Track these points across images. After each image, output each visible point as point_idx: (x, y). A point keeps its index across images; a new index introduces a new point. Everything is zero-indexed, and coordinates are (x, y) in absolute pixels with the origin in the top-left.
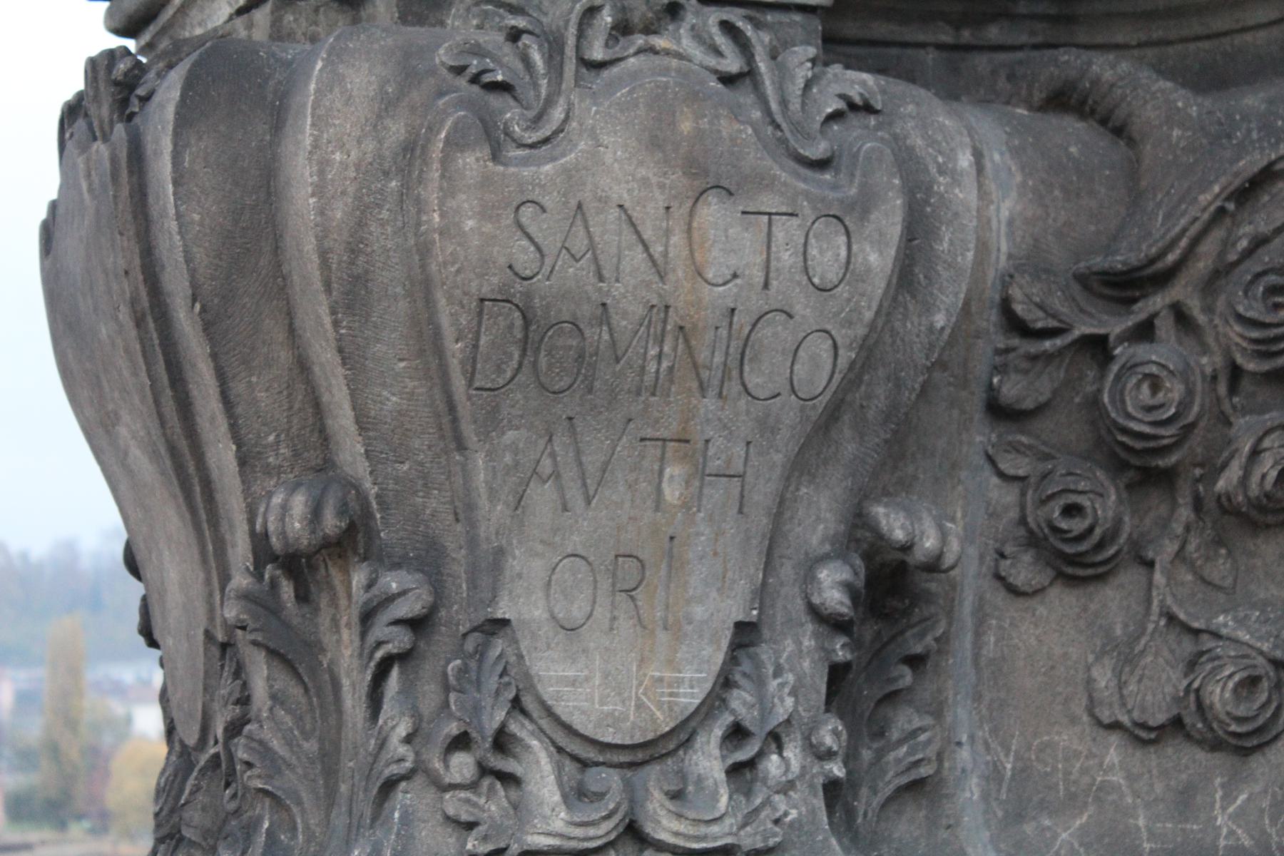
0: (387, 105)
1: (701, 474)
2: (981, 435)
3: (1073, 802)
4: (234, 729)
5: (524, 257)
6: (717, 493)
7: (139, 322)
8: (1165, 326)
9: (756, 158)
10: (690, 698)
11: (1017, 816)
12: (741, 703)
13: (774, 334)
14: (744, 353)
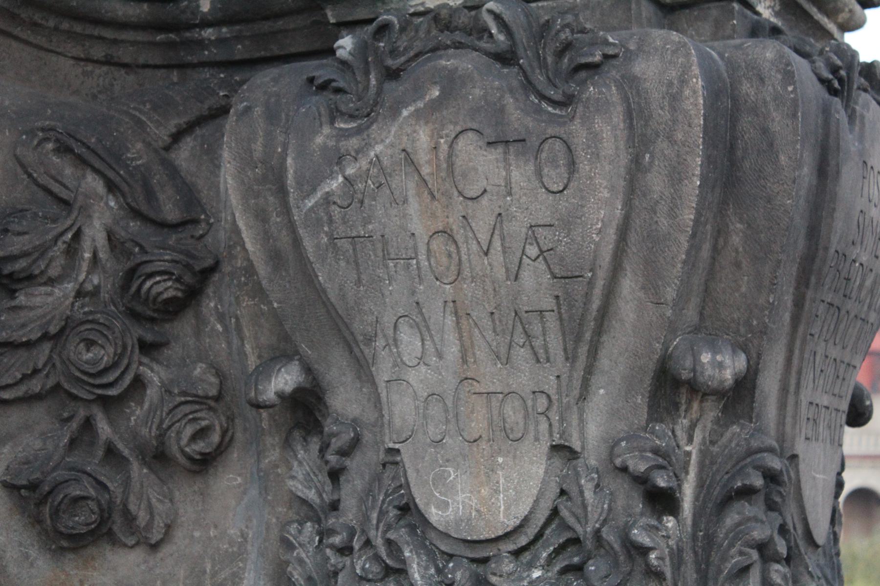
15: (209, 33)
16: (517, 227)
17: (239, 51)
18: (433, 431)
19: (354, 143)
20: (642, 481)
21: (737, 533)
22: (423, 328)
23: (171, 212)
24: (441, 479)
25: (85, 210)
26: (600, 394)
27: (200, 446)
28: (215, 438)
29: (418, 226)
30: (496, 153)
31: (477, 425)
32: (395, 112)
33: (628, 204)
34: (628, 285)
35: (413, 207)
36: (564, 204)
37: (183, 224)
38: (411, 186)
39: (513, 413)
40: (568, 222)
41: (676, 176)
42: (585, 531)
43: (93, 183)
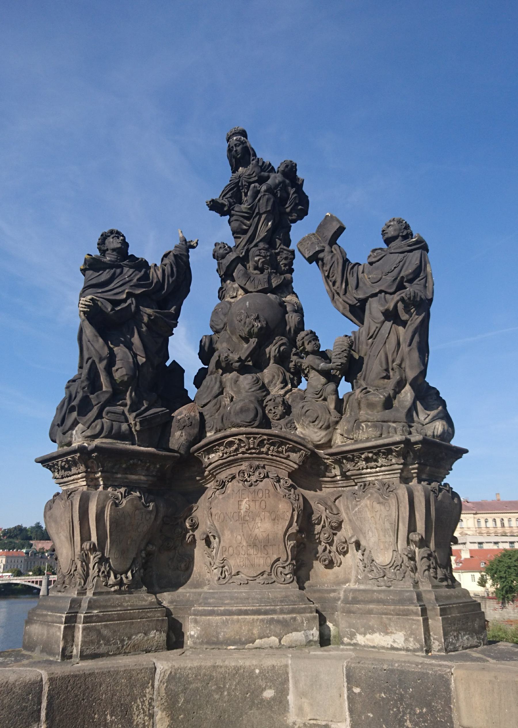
4: (75, 570)
7: (70, 523)
15: (340, 482)
16: (383, 516)
19: (358, 503)
23: (336, 513)
24: (378, 556)
28: (346, 548)
29: (369, 516)
30: (379, 505)
31: (382, 547)
32: (364, 498)
35: (368, 513)
37: (337, 514)
38: (367, 510)
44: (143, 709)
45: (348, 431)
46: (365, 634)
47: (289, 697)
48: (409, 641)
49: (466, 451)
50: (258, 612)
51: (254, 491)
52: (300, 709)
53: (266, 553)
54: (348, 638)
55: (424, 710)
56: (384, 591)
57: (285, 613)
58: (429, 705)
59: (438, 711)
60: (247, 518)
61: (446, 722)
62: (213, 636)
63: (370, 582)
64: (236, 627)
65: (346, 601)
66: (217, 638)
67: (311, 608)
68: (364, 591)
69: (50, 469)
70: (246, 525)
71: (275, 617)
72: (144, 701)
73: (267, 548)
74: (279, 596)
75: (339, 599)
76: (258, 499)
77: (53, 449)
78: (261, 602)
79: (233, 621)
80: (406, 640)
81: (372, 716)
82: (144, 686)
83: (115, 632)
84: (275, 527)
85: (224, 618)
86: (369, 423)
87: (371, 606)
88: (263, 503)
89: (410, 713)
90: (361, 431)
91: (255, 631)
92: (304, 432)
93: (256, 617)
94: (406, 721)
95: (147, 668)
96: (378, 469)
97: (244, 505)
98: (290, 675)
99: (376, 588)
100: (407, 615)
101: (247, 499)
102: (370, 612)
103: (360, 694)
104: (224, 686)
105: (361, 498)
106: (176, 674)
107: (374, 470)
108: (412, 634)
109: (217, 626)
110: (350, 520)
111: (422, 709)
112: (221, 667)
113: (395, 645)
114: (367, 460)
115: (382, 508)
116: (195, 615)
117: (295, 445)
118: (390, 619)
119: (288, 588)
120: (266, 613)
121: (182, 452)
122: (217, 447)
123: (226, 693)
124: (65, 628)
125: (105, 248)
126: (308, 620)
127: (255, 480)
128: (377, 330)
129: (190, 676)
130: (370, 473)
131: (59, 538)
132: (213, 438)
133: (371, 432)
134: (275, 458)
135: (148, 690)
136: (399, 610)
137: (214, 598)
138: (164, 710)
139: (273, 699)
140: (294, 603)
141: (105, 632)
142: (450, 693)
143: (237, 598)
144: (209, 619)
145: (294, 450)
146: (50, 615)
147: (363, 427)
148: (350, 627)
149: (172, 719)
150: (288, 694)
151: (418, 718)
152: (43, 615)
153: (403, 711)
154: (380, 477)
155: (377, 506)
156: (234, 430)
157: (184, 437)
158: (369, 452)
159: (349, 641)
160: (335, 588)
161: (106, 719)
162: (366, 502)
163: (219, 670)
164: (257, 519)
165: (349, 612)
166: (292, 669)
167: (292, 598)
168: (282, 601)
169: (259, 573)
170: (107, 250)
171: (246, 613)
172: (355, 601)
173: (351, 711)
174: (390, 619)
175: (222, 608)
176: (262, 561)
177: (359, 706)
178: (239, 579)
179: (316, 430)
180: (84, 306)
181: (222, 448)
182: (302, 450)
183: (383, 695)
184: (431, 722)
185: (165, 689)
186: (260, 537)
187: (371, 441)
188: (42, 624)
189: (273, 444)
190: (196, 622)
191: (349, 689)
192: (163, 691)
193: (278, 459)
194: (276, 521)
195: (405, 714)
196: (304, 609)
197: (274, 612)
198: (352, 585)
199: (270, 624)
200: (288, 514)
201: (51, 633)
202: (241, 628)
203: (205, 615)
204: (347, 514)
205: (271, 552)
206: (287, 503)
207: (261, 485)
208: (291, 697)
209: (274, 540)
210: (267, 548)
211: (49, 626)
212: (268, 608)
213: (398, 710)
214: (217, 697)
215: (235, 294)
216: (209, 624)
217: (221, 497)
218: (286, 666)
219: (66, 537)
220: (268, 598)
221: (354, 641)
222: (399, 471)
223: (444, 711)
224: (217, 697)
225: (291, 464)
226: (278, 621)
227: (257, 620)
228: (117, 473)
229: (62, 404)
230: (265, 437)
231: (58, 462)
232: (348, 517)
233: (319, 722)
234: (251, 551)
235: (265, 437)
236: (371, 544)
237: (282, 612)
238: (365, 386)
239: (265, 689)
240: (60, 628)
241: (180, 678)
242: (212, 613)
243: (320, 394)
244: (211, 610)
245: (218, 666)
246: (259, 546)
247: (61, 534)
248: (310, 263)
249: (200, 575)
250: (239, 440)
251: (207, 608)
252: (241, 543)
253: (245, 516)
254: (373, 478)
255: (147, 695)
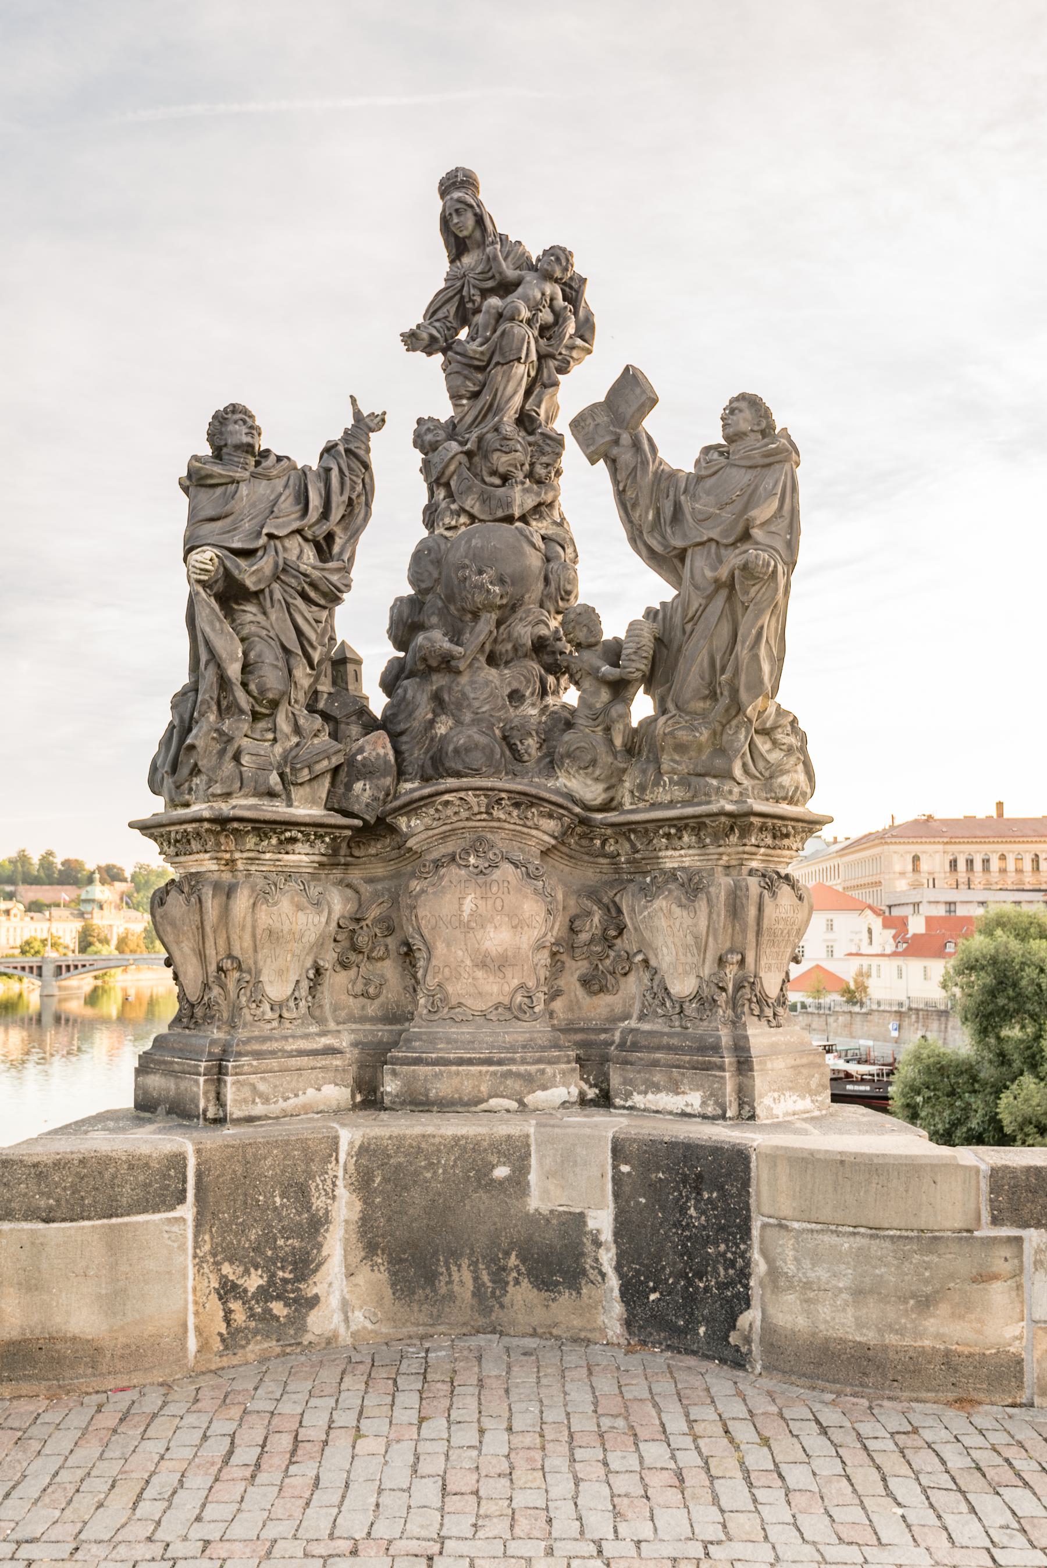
0: (250, 897)
1: (293, 955)
2: (333, 945)
3: (344, 1008)
5: (271, 922)
6: (296, 958)
8: (365, 928)
9: (307, 904)
10: (289, 993)
11: (335, 1011)
12: (297, 994)
13: (307, 933)
14: (302, 936)
16: (685, 926)
17: (632, 870)
18: (671, 971)
20: (717, 984)
21: (742, 996)
22: (667, 947)
25: (593, 915)
26: (707, 964)
27: (623, 972)
31: (680, 970)
33: (709, 921)
34: (711, 939)
36: (695, 920)
39: (688, 968)
40: (695, 925)
41: (719, 915)
42: (704, 996)
43: (595, 908)
44: (325, 1190)
45: (642, 788)
46: (646, 1093)
47: (529, 1177)
48: (708, 1105)
49: (831, 820)
50: (489, 1062)
51: (485, 883)
52: (545, 1193)
53: (501, 975)
54: (621, 1099)
55: (715, 1195)
56: (678, 1034)
57: (528, 1063)
58: (721, 1188)
59: (732, 1196)
60: (473, 925)
61: (742, 1209)
62: (421, 1094)
63: (660, 1020)
64: (455, 1081)
65: (622, 1046)
66: (427, 1096)
67: (568, 1056)
68: (650, 1033)
69: (156, 840)
70: (471, 935)
71: (514, 1068)
72: (325, 1180)
73: (503, 969)
74: (520, 1039)
75: (613, 1042)
76: (489, 895)
77: (155, 806)
78: (493, 1047)
79: (450, 1072)
80: (704, 1103)
81: (643, 1201)
82: (326, 1160)
83: (276, 1086)
84: (517, 938)
85: (437, 1069)
86: (675, 777)
87: (658, 1055)
88: (499, 902)
89: (695, 1199)
90: (661, 789)
91: (484, 1088)
92: (569, 784)
93: (484, 1068)
94: (690, 1208)
95: (328, 1137)
96: (682, 852)
97: (468, 905)
98: (533, 1148)
99: (667, 1030)
100: (707, 1070)
101: (473, 895)
102: (655, 1064)
103: (629, 1174)
104: (439, 1162)
105: (654, 896)
106: (369, 1144)
107: (677, 853)
108: (712, 1095)
109: (425, 1080)
110: (635, 929)
111: (711, 1193)
112: (434, 1136)
113: (688, 1110)
114: (668, 836)
115: (685, 913)
116: (392, 1064)
117: (553, 808)
118: (683, 1074)
119: (535, 1027)
120: (500, 1063)
121: (367, 817)
122: (424, 809)
123: (440, 1171)
124: (206, 1081)
125: (222, 443)
126: (564, 1073)
127: (486, 865)
128: (701, 608)
129: (390, 1147)
130: (671, 857)
131: (181, 949)
132: (417, 795)
133: (677, 793)
134: (519, 828)
135: (330, 1166)
136: (697, 1061)
137: (421, 1040)
138: (354, 1191)
139: (508, 1179)
140: (543, 1048)
141: (262, 1087)
142: (749, 1173)
143: (456, 1041)
144: (414, 1071)
145: (550, 816)
146: (177, 1063)
147: (665, 782)
148: (624, 1083)
149: (365, 1203)
150: (529, 1173)
151: (706, 1205)
152: (165, 1062)
153: (687, 1196)
154: (687, 864)
155: (677, 911)
156: (451, 782)
157: (368, 793)
158: (670, 826)
159: (622, 1103)
160: (607, 1026)
161: (274, 1203)
162: (660, 903)
163: (432, 1140)
164: (489, 925)
165: (626, 1062)
166: (536, 1140)
167: (540, 1042)
168: (524, 1047)
169: (490, 1004)
170: (226, 445)
171: (470, 1062)
172: (635, 1047)
173: (616, 1195)
174: (683, 1074)
175: (434, 1056)
176: (495, 989)
177: (627, 1189)
178: (461, 1014)
179: (589, 782)
180: (198, 571)
181: (432, 811)
182: (564, 816)
183: (661, 1175)
184: (723, 1210)
185: (355, 1165)
186: (494, 953)
187: (674, 808)
188: (166, 1075)
189: (517, 805)
190: (394, 1073)
191: (615, 1167)
192: (351, 1168)
193: (525, 830)
194: (519, 929)
195: (688, 1199)
196: (558, 1057)
197: (513, 1061)
198: (633, 1023)
199: (506, 1078)
200: (538, 918)
201: (182, 1088)
202: (462, 1084)
203: (409, 1064)
204: (631, 919)
205: (509, 975)
206: (537, 901)
207: (497, 874)
208: (532, 1177)
209: (514, 957)
210: (503, 969)
211: (178, 1077)
212: (503, 1055)
213: (681, 1194)
214: (429, 1175)
215: (453, 523)
216: (414, 1077)
217: (430, 890)
218: (528, 1136)
219: (194, 950)
220: (504, 1042)
221: (629, 1103)
222: (716, 857)
223: (740, 1195)
224: (429, 1175)
225: (546, 838)
226: (518, 1075)
227: (487, 1072)
228: (264, 853)
229: (168, 734)
230: (504, 795)
231: (170, 832)
232: (633, 924)
233: (572, 1210)
234: (480, 974)
235: (504, 795)
236: (664, 966)
237: (524, 1062)
238: (674, 712)
239: (493, 1167)
240: (197, 1082)
241: (375, 1151)
242: (417, 1062)
243: (600, 719)
244: (417, 1058)
245: (429, 1136)
246: (492, 966)
247: (183, 945)
248: (593, 462)
249: (398, 1006)
250: (461, 799)
251: (410, 1054)
252: (462, 961)
253: (469, 921)
254: (676, 865)
255: (330, 1172)
